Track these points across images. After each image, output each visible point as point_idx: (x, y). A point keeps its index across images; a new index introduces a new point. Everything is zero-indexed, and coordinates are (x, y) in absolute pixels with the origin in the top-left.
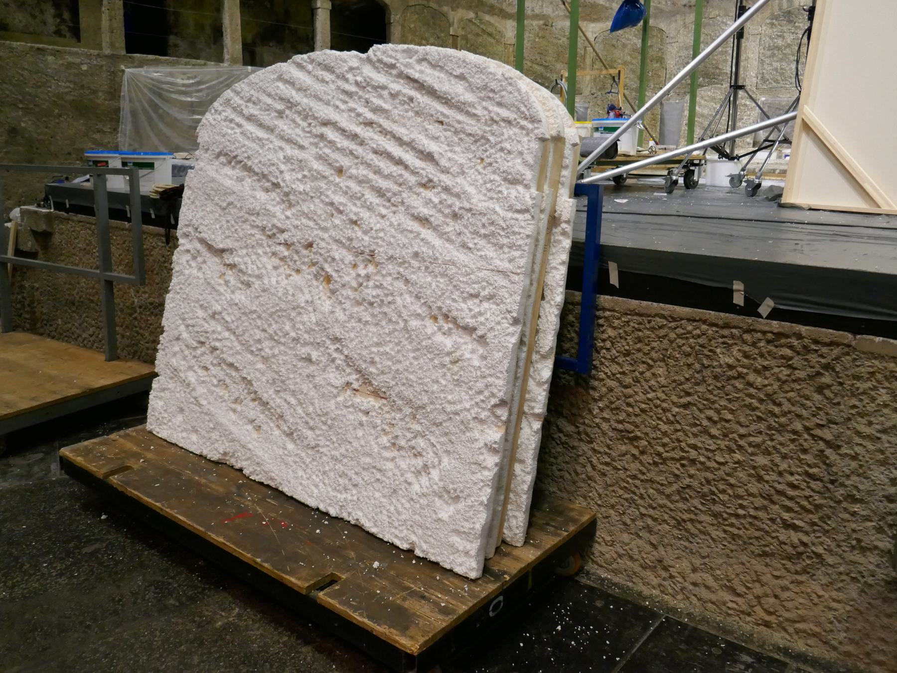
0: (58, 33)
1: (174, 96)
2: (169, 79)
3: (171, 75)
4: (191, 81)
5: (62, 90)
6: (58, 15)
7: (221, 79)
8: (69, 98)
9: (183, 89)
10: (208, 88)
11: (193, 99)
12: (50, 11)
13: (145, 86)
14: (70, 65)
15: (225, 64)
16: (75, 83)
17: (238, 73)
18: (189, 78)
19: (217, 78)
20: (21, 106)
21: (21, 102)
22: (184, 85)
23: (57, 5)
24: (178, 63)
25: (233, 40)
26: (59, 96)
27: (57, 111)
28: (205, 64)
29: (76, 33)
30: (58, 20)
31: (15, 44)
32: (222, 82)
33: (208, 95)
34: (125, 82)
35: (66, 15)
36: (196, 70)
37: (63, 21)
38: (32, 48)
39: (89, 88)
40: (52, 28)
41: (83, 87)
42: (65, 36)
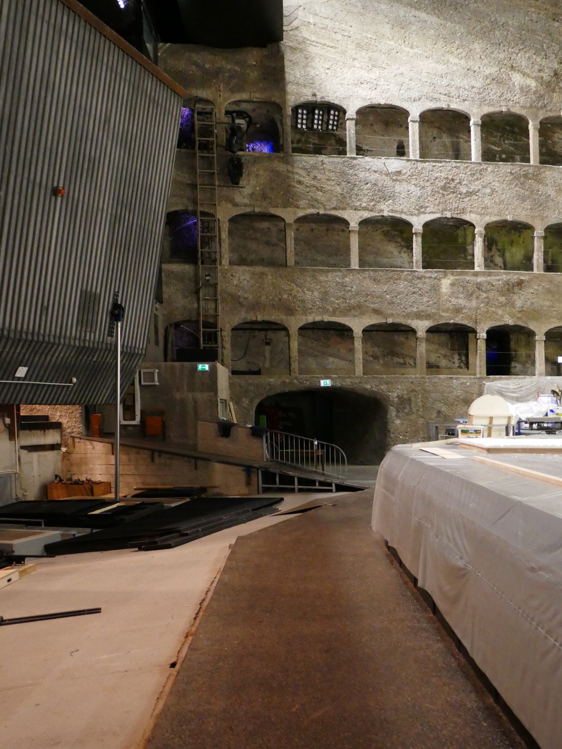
0: (460, 367)
1: (508, 394)
2: (507, 386)
3: (507, 384)
4: (517, 386)
5: (459, 394)
6: (460, 359)
7: (533, 384)
8: (462, 397)
9: (513, 390)
10: (526, 389)
11: (518, 395)
12: (457, 357)
13: (495, 390)
14: (462, 383)
15: (536, 377)
16: (464, 391)
17: (542, 380)
18: (516, 385)
19: (531, 384)
20: (442, 401)
21: (443, 400)
22: (513, 389)
23: (460, 355)
24: (511, 378)
25: (540, 364)
26: (458, 397)
27: (456, 403)
28: (525, 378)
29: (467, 366)
30: (460, 361)
31: (441, 376)
32: (533, 386)
33: (525, 393)
34: (485, 389)
35: (464, 358)
36: (520, 381)
37: (462, 361)
38: (448, 377)
39: (470, 392)
40: (457, 365)
41: (467, 392)
42: (462, 368)
